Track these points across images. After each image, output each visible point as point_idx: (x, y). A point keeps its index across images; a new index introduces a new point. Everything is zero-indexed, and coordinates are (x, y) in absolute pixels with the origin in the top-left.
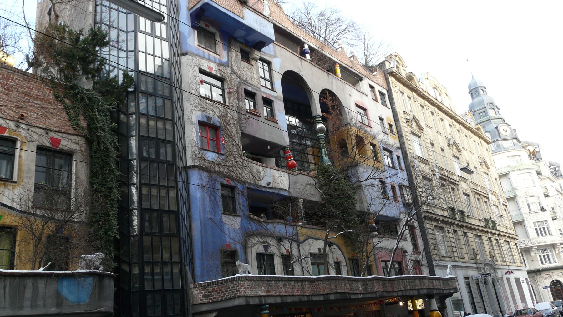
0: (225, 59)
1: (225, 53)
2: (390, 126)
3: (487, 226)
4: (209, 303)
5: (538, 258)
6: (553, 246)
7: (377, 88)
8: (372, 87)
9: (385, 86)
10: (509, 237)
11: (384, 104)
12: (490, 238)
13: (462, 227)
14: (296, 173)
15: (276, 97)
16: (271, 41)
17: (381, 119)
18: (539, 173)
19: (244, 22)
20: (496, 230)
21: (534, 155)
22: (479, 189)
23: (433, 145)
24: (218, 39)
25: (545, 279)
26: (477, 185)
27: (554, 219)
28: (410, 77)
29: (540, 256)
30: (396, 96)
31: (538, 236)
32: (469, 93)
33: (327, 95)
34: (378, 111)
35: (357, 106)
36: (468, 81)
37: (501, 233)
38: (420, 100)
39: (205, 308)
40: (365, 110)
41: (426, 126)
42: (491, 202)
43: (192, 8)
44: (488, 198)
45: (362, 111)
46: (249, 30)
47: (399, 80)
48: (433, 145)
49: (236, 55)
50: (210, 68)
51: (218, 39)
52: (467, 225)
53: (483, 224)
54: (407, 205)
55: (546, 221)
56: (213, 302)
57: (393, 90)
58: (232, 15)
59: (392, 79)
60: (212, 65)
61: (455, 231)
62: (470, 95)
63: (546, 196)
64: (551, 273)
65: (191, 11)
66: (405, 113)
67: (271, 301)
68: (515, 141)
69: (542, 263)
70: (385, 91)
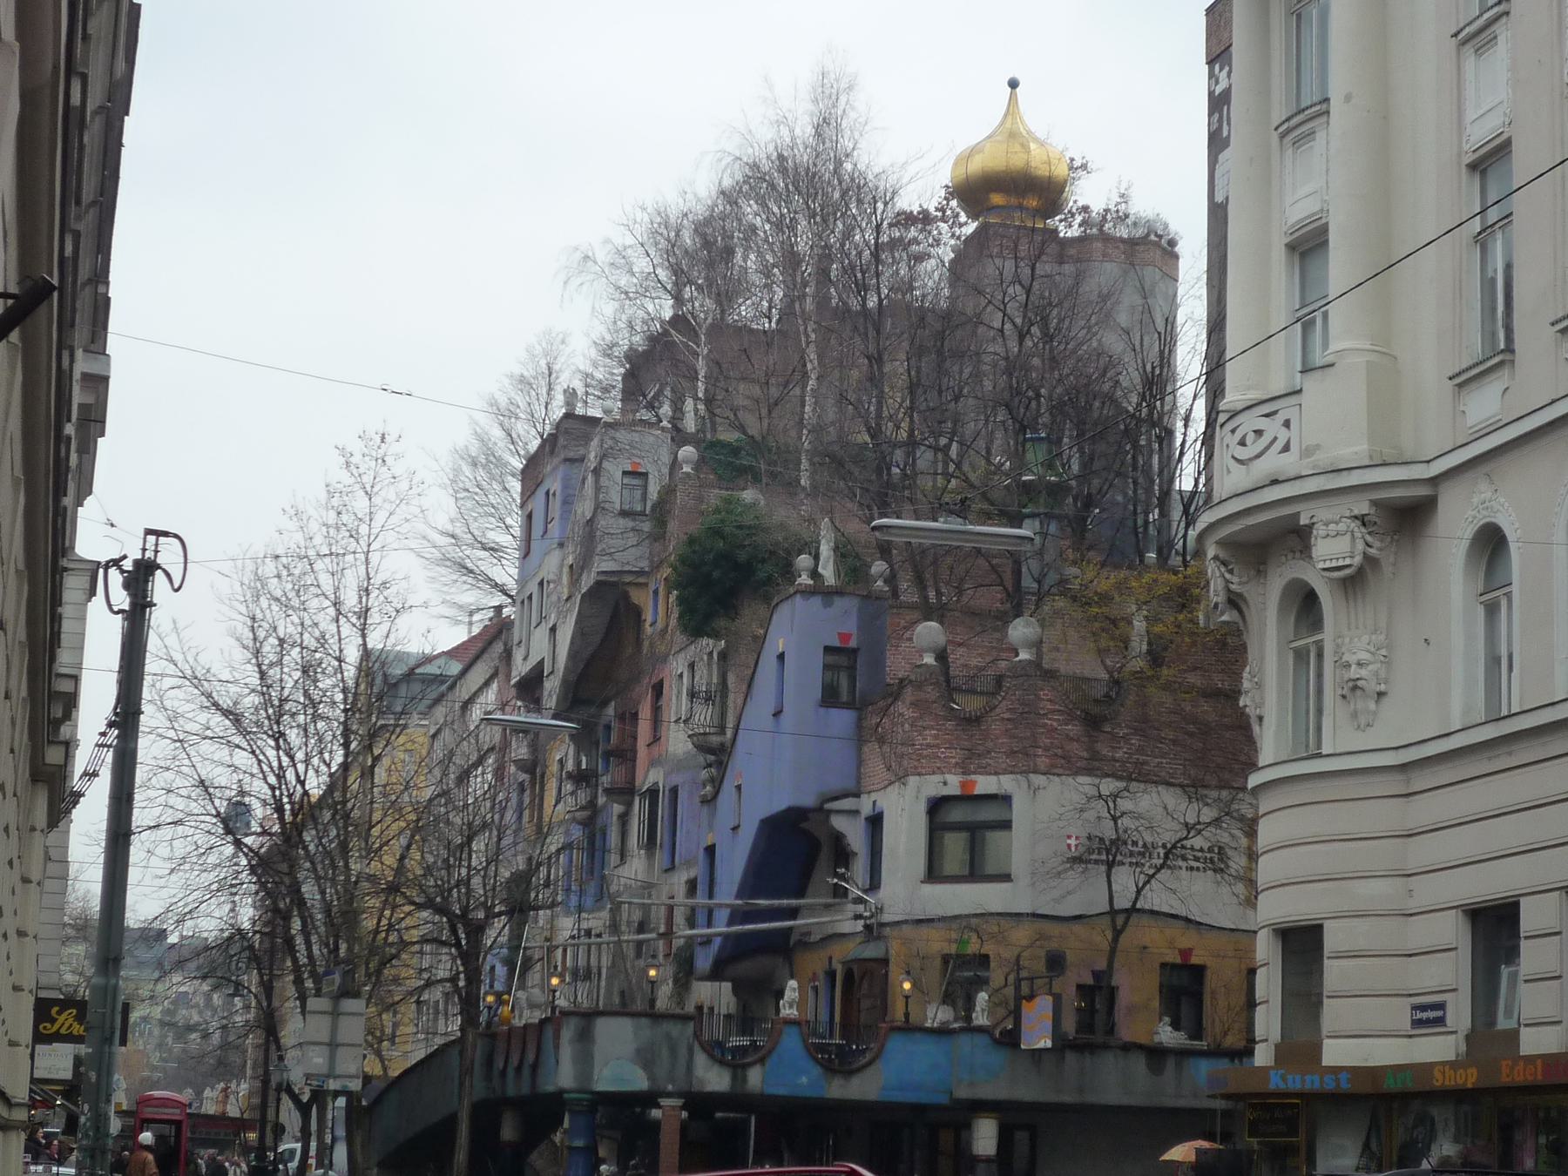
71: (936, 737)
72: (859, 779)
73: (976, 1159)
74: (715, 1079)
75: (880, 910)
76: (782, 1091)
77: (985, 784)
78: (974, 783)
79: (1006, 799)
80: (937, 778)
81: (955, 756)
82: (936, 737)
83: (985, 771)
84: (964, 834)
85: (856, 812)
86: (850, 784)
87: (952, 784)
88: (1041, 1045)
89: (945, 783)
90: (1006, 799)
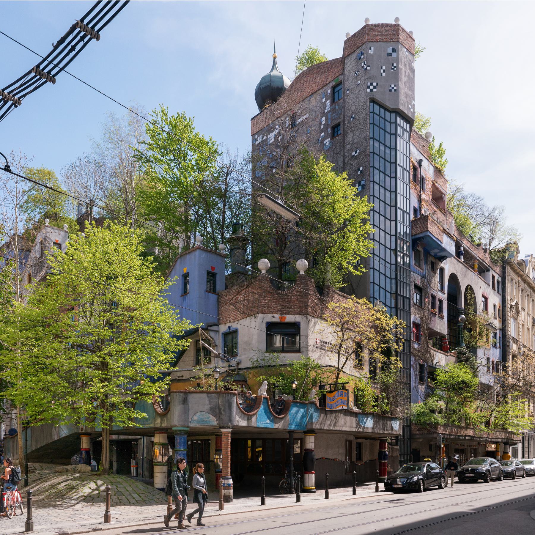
0: (424, 273)
1: (424, 267)
7: (497, 277)
8: (493, 277)
9: (501, 275)
11: (498, 292)
16: (451, 255)
17: (495, 306)
19: (443, 245)
24: (422, 256)
28: (521, 264)
30: (508, 285)
33: (469, 288)
34: (494, 299)
35: (483, 296)
38: (522, 284)
40: (486, 299)
43: (415, 235)
45: (484, 300)
46: (444, 250)
47: (513, 269)
49: (429, 267)
50: (418, 282)
51: (422, 256)
57: (508, 278)
58: (438, 241)
60: (420, 277)
65: (414, 237)
70: (500, 280)
77: (290, 318)
80: (271, 315)
81: (278, 307)
83: (289, 313)
87: (277, 318)
89: (274, 317)
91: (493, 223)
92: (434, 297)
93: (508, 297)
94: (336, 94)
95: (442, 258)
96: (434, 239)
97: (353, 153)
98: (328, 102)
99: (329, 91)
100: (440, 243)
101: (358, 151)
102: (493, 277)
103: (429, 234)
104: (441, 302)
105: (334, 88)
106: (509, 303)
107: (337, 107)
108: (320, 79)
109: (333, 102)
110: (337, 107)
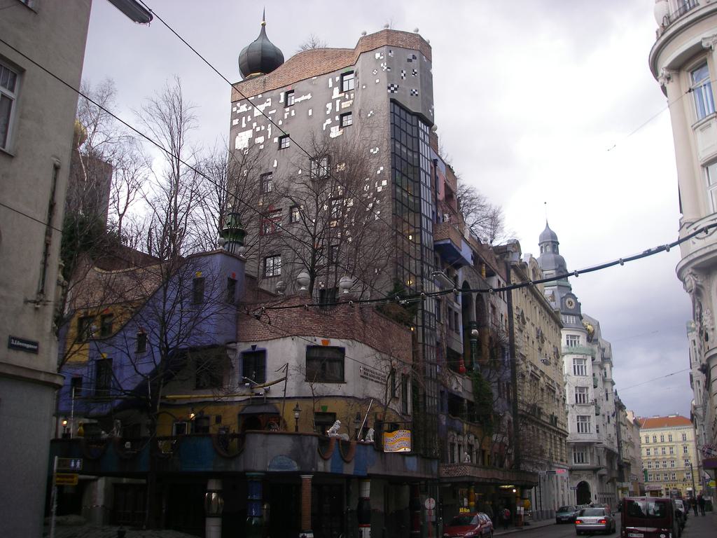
2: (506, 321)
3: (552, 423)
4: (448, 478)
5: (573, 455)
6: (590, 444)
8: (499, 282)
10: (563, 434)
12: (551, 435)
13: (537, 423)
14: (465, 377)
15: (459, 310)
16: (468, 264)
17: (502, 316)
18: (593, 359)
20: (556, 426)
21: (591, 337)
22: (550, 382)
23: (528, 338)
25: (575, 479)
26: (549, 379)
27: (597, 415)
28: (524, 266)
29: (575, 454)
31: (579, 431)
32: (539, 245)
36: (543, 228)
37: (560, 431)
39: (445, 480)
41: (527, 318)
42: (556, 397)
44: (554, 392)
48: (528, 338)
52: (540, 421)
53: (548, 421)
54: (509, 402)
55: (589, 417)
56: (451, 478)
59: (512, 272)
61: (533, 427)
62: (539, 248)
63: (595, 387)
64: (581, 473)
66: (517, 308)
67: (476, 480)
68: (578, 318)
69: (575, 461)
71: (311, 321)
72: (237, 335)
73: (362, 500)
74: (321, 466)
75: (267, 391)
76: (335, 471)
77: (335, 342)
78: (329, 341)
79: (341, 350)
82: (311, 321)
84: (323, 364)
85: (235, 350)
86: (232, 338)
87: (319, 341)
88: (402, 450)
89: (315, 340)
90: (341, 350)
91: (494, 221)
92: (450, 310)
93: (514, 306)
94: (345, 84)
95: (458, 266)
96: (455, 247)
97: (372, 150)
98: (336, 90)
99: (338, 79)
100: (459, 251)
101: (377, 149)
102: (499, 282)
103: (449, 242)
104: (456, 314)
105: (343, 75)
106: (515, 311)
107: (347, 96)
108: (326, 65)
109: (341, 91)
110: (347, 96)
